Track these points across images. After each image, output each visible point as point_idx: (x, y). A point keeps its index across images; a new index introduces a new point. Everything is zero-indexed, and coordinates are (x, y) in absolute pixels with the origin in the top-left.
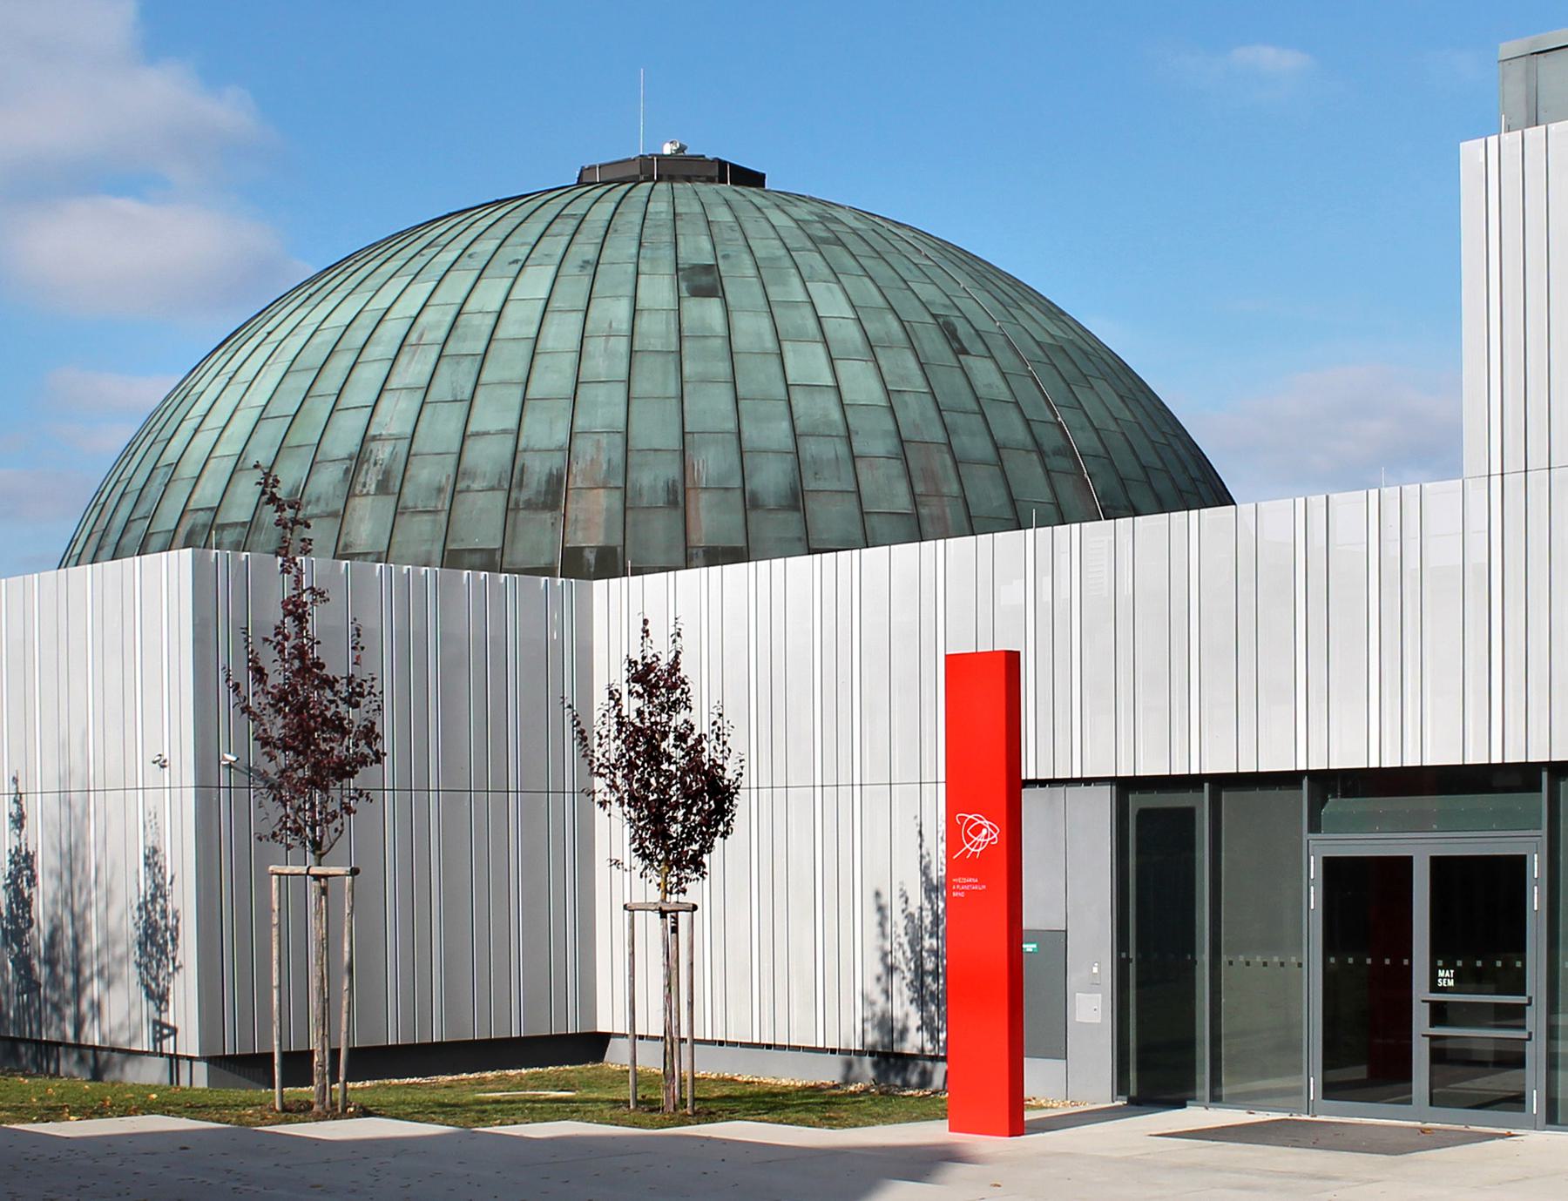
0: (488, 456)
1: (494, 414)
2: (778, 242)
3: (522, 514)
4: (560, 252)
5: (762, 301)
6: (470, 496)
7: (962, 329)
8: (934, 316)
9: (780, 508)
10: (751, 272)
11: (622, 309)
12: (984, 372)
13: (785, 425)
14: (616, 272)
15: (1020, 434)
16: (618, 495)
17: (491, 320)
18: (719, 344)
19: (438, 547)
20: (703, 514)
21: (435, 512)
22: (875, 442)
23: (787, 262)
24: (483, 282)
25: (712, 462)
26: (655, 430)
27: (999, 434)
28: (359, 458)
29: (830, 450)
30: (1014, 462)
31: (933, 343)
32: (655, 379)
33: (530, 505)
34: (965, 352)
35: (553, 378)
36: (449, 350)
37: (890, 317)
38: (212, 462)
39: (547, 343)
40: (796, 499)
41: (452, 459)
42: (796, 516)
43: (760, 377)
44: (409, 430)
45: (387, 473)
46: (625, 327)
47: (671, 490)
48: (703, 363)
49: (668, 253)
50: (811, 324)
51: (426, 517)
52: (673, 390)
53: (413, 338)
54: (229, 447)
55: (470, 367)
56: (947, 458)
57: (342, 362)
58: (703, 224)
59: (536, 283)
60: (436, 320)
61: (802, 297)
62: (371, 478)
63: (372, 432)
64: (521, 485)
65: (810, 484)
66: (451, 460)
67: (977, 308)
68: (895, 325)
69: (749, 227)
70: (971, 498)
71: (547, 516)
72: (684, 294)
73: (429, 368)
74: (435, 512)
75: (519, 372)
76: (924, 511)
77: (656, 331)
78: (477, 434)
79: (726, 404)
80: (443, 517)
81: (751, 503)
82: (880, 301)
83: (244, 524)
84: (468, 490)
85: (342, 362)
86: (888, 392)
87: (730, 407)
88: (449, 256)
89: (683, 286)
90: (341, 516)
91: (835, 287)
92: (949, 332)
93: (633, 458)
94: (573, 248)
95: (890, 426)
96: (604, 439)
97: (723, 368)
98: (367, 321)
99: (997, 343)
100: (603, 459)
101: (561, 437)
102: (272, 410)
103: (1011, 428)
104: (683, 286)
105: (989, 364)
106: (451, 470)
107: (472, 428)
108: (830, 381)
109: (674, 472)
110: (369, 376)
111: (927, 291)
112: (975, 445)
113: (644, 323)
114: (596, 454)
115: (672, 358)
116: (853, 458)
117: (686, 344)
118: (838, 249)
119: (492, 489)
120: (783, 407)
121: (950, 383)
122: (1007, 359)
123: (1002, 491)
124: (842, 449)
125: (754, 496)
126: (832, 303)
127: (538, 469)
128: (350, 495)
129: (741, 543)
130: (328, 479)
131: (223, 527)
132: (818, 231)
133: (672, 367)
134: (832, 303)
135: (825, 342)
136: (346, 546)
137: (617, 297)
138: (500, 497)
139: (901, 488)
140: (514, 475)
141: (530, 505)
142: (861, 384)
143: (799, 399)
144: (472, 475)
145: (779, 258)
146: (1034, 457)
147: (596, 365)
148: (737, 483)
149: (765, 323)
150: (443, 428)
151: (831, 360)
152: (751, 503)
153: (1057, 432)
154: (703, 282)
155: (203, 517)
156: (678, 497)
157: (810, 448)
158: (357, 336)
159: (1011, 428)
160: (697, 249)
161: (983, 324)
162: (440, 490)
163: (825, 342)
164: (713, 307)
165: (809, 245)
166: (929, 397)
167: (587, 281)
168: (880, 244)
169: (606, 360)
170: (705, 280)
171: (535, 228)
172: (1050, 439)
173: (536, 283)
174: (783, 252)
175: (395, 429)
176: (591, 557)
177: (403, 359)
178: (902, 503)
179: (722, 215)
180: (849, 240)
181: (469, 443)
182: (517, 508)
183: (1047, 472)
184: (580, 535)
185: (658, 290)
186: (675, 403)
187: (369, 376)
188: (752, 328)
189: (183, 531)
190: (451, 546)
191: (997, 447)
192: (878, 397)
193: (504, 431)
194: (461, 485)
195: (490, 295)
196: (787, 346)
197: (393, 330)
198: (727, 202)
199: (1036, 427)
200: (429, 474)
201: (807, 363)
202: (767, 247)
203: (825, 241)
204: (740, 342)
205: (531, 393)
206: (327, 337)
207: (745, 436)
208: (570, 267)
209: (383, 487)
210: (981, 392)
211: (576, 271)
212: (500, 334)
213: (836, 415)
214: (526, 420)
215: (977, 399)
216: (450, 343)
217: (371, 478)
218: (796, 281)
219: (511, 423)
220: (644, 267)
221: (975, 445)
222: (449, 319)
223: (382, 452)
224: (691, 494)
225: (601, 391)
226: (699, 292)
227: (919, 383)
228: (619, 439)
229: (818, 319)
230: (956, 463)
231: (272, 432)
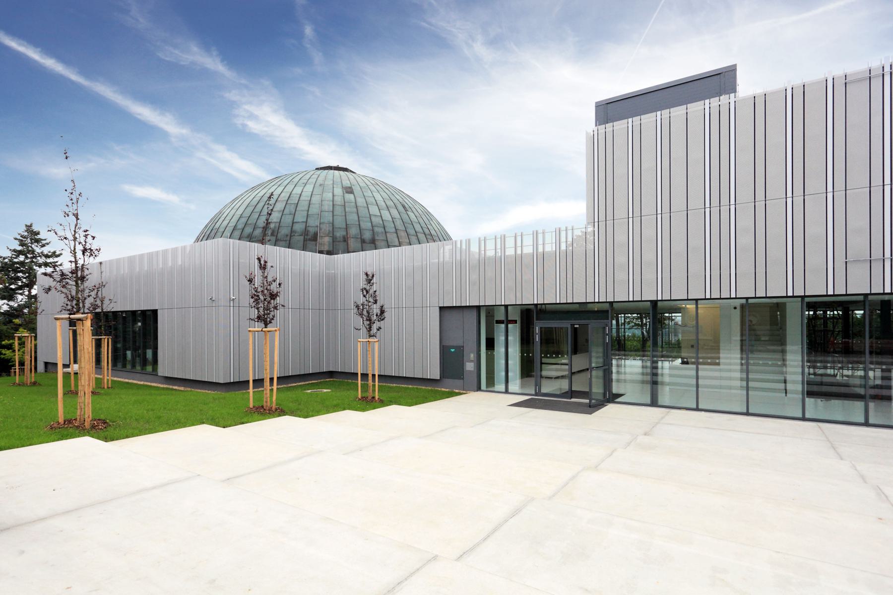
0: (299, 228)
1: (300, 217)
11: (330, 195)
25: (353, 231)
28: (265, 228)
29: (381, 230)
32: (339, 211)
33: (310, 240)
43: (363, 212)
47: (344, 237)
54: (232, 224)
55: (293, 207)
65: (377, 238)
66: (290, 229)
75: (306, 208)
79: (356, 218)
92: (404, 207)
109: (345, 233)
113: (336, 198)
114: (326, 228)
121: (405, 217)
127: (312, 230)
138: (302, 238)
142: (386, 215)
150: (288, 220)
157: (376, 229)
164: (351, 196)
169: (327, 206)
172: (427, 231)
175: (275, 220)
185: (338, 191)
188: (361, 201)
192: (390, 219)
195: (298, 190)
201: (374, 210)
204: (358, 204)
206: (257, 199)
209: (272, 234)
217: (269, 232)
221: (412, 232)
231: (243, 220)
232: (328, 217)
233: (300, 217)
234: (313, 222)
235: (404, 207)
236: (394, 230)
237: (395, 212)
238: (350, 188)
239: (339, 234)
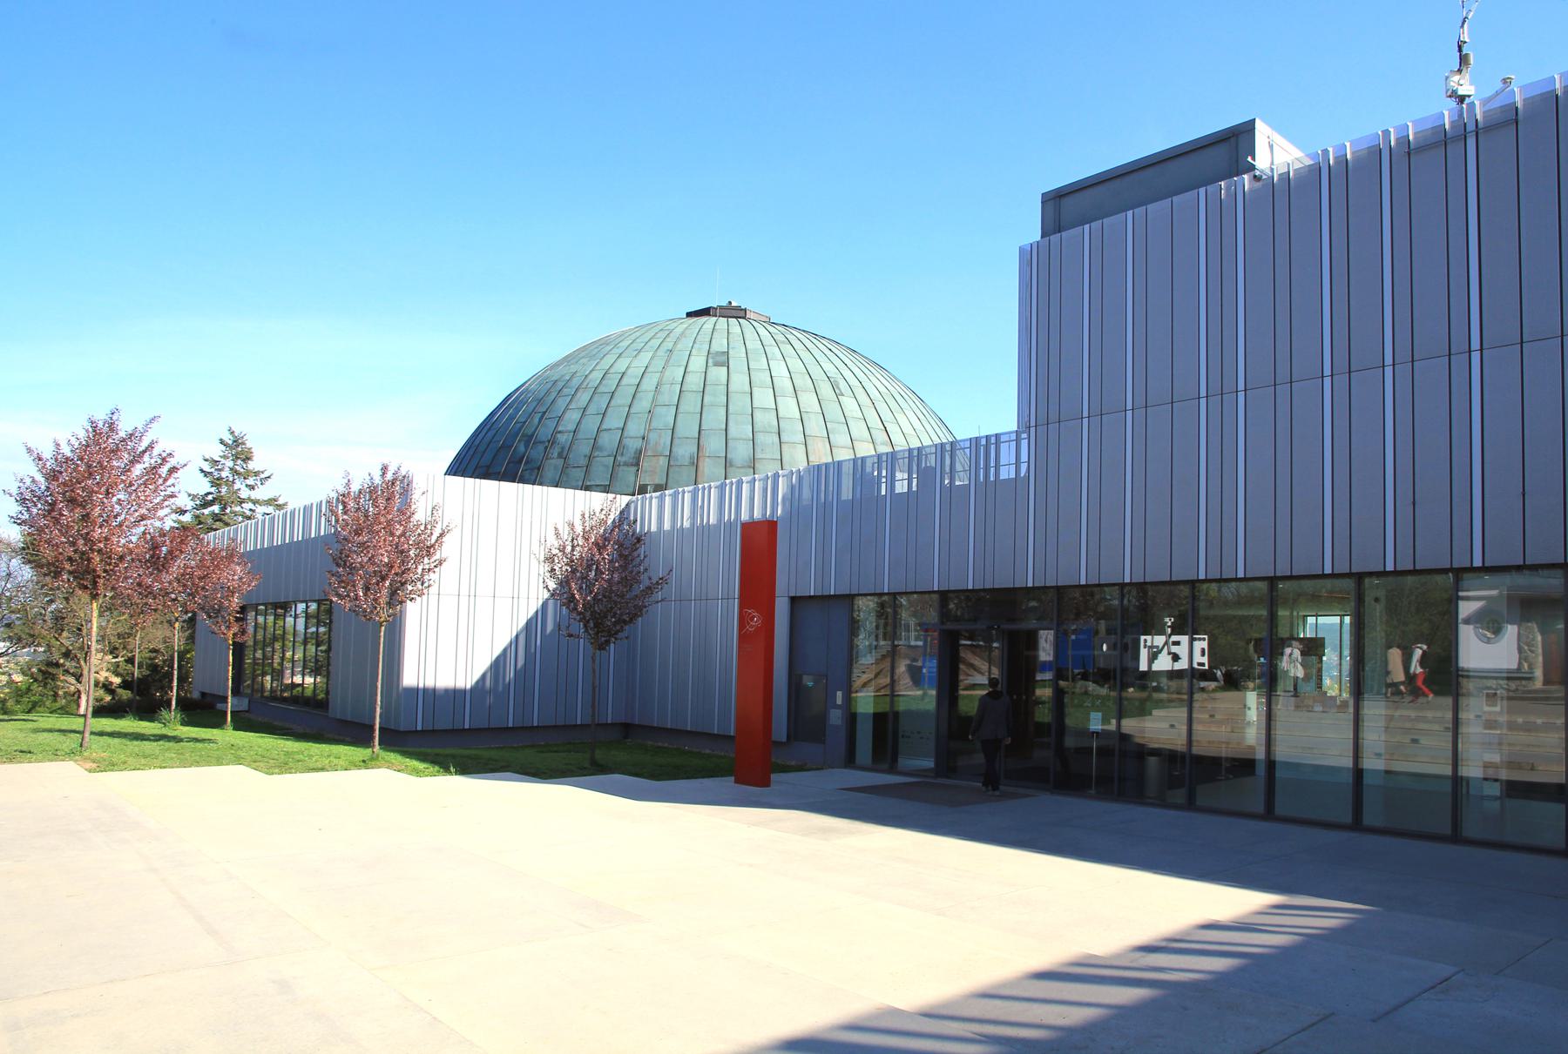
0: (609, 441)
25: (714, 444)
26: (687, 428)
31: (826, 390)
32: (691, 404)
33: (626, 464)
39: (643, 387)
43: (739, 403)
47: (691, 457)
48: (716, 397)
60: (597, 375)
77: (694, 381)
92: (834, 386)
93: (676, 441)
113: (689, 378)
127: (633, 445)
141: (626, 464)
143: (757, 415)
144: (600, 449)
150: (591, 424)
157: (760, 438)
160: (720, 344)
173: (645, 358)
185: (698, 363)
188: (739, 381)
200: (584, 448)
208: (661, 353)
209: (560, 455)
226: (717, 364)
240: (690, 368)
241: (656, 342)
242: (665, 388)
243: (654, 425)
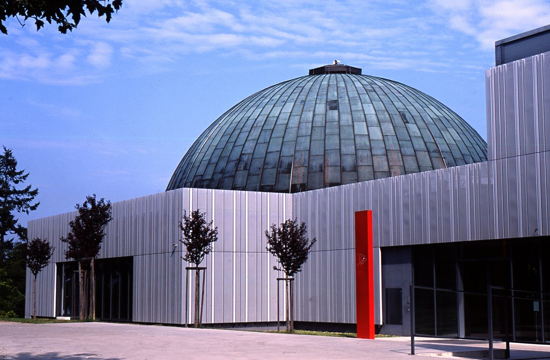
0: (272, 158)
1: (274, 147)
2: (356, 92)
3: (281, 175)
4: (296, 98)
5: (349, 110)
6: (267, 170)
7: (408, 116)
8: (399, 112)
9: (351, 171)
10: (347, 102)
11: (311, 114)
12: (413, 128)
13: (353, 147)
14: (310, 104)
15: (423, 147)
16: (307, 168)
17: (275, 119)
18: (336, 123)
19: (258, 185)
20: (329, 174)
21: (258, 175)
22: (379, 151)
23: (358, 98)
24: (275, 108)
25: (333, 158)
26: (318, 150)
27: (416, 147)
28: (240, 160)
29: (367, 153)
30: (420, 155)
31: (398, 120)
32: (318, 135)
33: (283, 172)
34: (408, 122)
35: (291, 135)
36: (264, 128)
37: (386, 113)
38: (202, 162)
39: (290, 125)
40: (355, 169)
41: (263, 160)
42: (356, 173)
43: (347, 132)
44: (252, 152)
45: (246, 164)
46: (311, 119)
47: (321, 167)
49: (325, 97)
50: (363, 116)
51: (256, 176)
52: (323, 138)
53: (255, 125)
55: (269, 133)
56: (400, 154)
57: (237, 132)
58: (336, 88)
59: (289, 107)
60: (262, 119)
61: (361, 109)
62: (242, 166)
63: (243, 152)
64: (281, 167)
67: (413, 108)
68: (387, 116)
69: (349, 87)
70: (406, 166)
71: (287, 175)
72: (328, 109)
73: (258, 134)
74: (258, 175)
75: (282, 134)
76: (392, 170)
77: (319, 120)
78: (270, 152)
79: (337, 141)
80: (260, 176)
81: (343, 170)
82: (384, 108)
83: (209, 180)
84: (267, 168)
85: (237, 132)
86: (383, 135)
87: (338, 142)
88: (267, 100)
89: (328, 107)
90: (234, 177)
91: (371, 105)
92: (403, 116)
93: (311, 158)
94: (300, 97)
95: (384, 146)
96: (303, 153)
97: (337, 131)
98: (244, 120)
99: (418, 119)
100: (303, 157)
101: (292, 152)
102: (218, 147)
103: (419, 144)
104: (328, 107)
105: (415, 125)
106: (262, 163)
107: (269, 151)
108: (367, 133)
109: (322, 161)
110: (243, 136)
111: (398, 104)
112: (409, 151)
113: (316, 118)
114: (303, 157)
115: (323, 128)
116: (372, 155)
117: (327, 124)
118: (374, 93)
119: (273, 168)
120: (353, 141)
121: (402, 132)
122: (421, 124)
123: (416, 164)
124: (369, 153)
125: (343, 167)
126: (370, 110)
127: (286, 161)
128: (237, 170)
129: (340, 182)
130: (232, 165)
131: (204, 180)
132: (369, 88)
133: (323, 131)
134: (370, 110)
135: (366, 122)
136: (235, 185)
137: (310, 111)
138: (275, 170)
139: (386, 163)
140: (280, 163)
141: (283, 172)
142: (376, 133)
143: (358, 140)
145: (356, 97)
146: (427, 153)
147: (303, 131)
148: (339, 164)
149: (350, 117)
150: (261, 150)
151: (367, 127)
152: (343, 170)
153: (435, 145)
154: (333, 105)
155: (199, 178)
156: (322, 169)
157: (360, 153)
158: (241, 125)
159: (419, 144)
160: (333, 95)
161: (415, 113)
162: (260, 168)
163: (366, 122)
164: (336, 113)
165: (365, 92)
166: (395, 137)
167: (302, 106)
168: (387, 91)
169: (306, 130)
170: (334, 105)
171: (291, 91)
172: (432, 147)
173: (289, 107)
174: (357, 95)
176: (298, 186)
177: (252, 131)
178: (386, 168)
179: (342, 84)
180: (377, 90)
181: (268, 155)
182: (279, 173)
183: (430, 158)
184: (296, 180)
185: (321, 108)
186: (323, 141)
187: (243, 136)
188: (346, 118)
189: (194, 182)
190: (262, 185)
191: (415, 151)
192: (381, 137)
193: (277, 151)
194: (265, 167)
195: (276, 112)
196: (355, 123)
197: (250, 123)
198: (344, 81)
199: (428, 144)
200: (257, 164)
201: (361, 128)
202: (353, 94)
203: (370, 91)
204: (342, 123)
205: (285, 140)
206: (234, 125)
207: (342, 150)
208: (298, 103)
209: (245, 168)
210: (412, 134)
211: (299, 104)
212: (278, 123)
213: (368, 143)
214: (283, 147)
215: (410, 136)
216: (265, 126)
217: (242, 166)
218: (360, 104)
219: (279, 149)
220: (318, 102)
221: (409, 151)
222: (265, 119)
223: (245, 158)
224: (326, 168)
225: (303, 138)
226: (332, 108)
227: (393, 133)
228: (307, 152)
229: (365, 115)
230: (402, 156)
231: (218, 152)
232: (305, 143)
233: (274, 147)
234: (288, 151)
235: (403, 116)
236: (383, 151)
237: (388, 127)
238: (336, 101)
239: (316, 163)
240: (317, 112)
241: (294, 96)
242: (303, 125)
243: (297, 148)
